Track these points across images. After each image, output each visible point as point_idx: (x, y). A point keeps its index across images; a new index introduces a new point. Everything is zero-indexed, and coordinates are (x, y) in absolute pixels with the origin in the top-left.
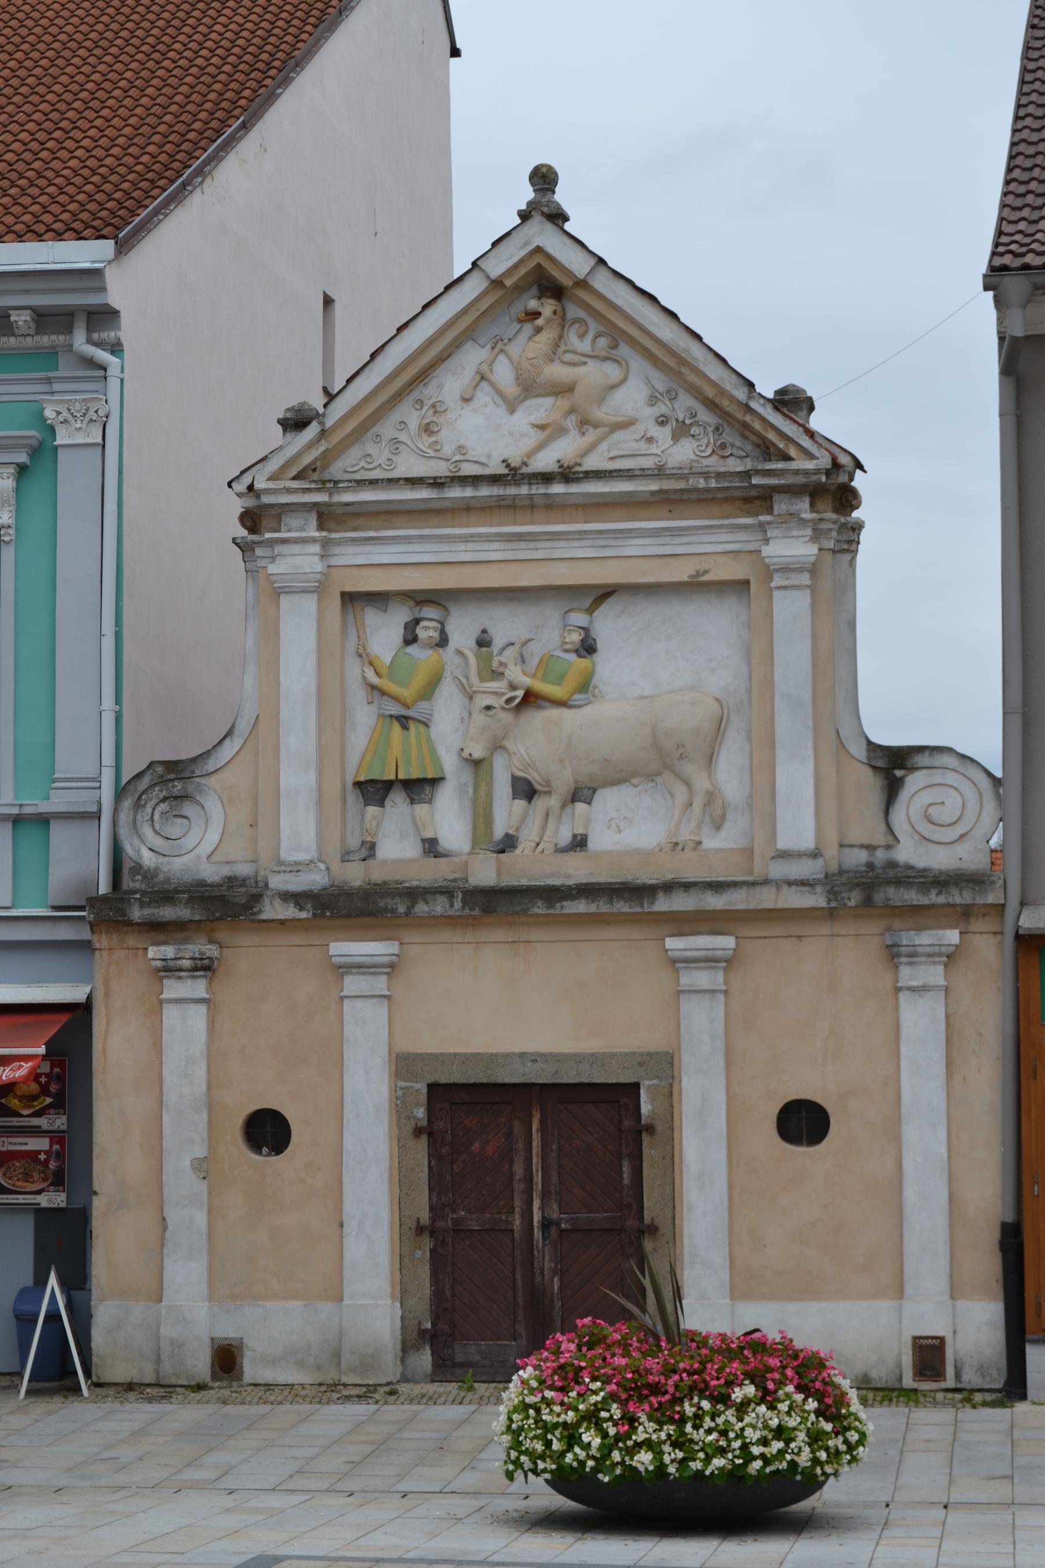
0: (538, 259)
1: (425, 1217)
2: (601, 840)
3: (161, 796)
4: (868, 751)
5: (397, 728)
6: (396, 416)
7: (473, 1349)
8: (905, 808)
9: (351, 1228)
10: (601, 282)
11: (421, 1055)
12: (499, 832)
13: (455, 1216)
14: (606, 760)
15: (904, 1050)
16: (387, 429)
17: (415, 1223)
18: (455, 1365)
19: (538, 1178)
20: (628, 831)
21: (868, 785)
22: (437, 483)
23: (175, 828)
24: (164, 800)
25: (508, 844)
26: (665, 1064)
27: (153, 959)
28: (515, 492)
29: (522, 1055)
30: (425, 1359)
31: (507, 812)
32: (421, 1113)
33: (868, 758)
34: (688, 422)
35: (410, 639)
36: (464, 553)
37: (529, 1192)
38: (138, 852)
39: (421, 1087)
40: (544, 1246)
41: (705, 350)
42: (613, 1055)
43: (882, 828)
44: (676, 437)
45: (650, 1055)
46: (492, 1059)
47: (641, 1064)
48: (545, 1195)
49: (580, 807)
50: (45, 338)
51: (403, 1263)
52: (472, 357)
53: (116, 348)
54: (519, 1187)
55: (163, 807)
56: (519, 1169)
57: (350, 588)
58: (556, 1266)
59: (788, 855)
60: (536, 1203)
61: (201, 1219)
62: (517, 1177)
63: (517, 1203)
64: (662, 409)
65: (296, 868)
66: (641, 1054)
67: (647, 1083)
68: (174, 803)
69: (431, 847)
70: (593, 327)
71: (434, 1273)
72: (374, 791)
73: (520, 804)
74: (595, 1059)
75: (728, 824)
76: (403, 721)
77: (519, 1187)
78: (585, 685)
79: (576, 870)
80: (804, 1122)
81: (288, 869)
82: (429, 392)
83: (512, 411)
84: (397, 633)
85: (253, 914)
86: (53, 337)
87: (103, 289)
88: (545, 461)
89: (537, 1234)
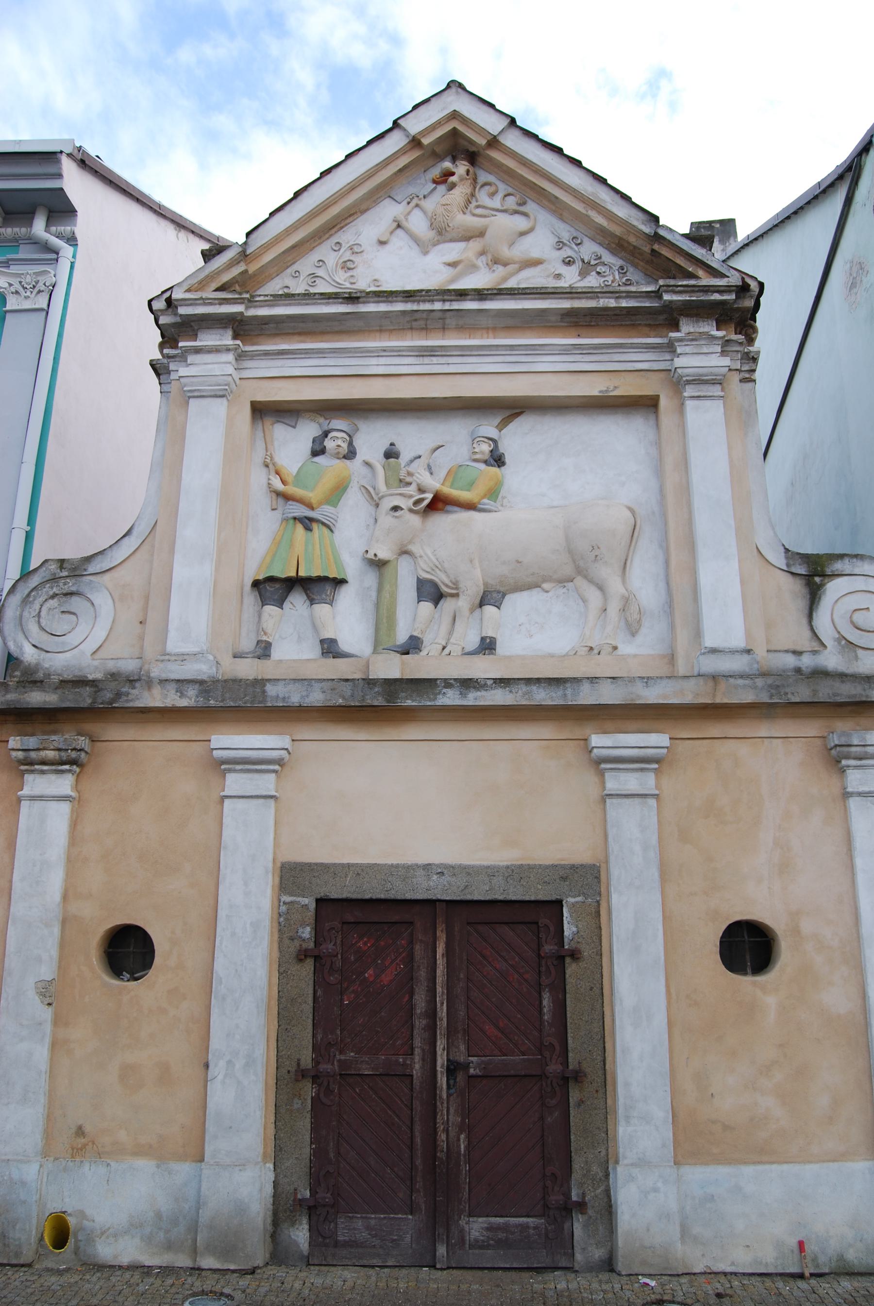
0: (454, 124)
1: (307, 1057)
3: (51, 593)
4: (787, 558)
5: (300, 528)
6: (314, 257)
7: (359, 1224)
8: (829, 613)
9: (218, 1069)
10: (512, 140)
11: (310, 865)
12: (402, 637)
13: (343, 1057)
14: (518, 562)
15: (859, 862)
17: (295, 1064)
18: (336, 1244)
19: (443, 1012)
20: (538, 634)
21: (791, 590)
23: (60, 625)
24: (53, 597)
25: (412, 646)
26: (590, 878)
27: (13, 750)
29: (427, 867)
30: (300, 1235)
31: (411, 616)
32: (307, 932)
33: (788, 565)
34: (593, 262)
35: (318, 451)
36: (376, 366)
37: (432, 1028)
38: (21, 648)
39: (309, 901)
40: (449, 1095)
41: (612, 193)
42: (531, 867)
43: (807, 633)
44: (583, 274)
45: (573, 868)
47: (564, 879)
48: (451, 1033)
49: (489, 610)
50: (9, 230)
51: (281, 1113)
52: (388, 211)
53: (72, 240)
54: (420, 1023)
55: (53, 603)
56: (420, 1001)
57: (260, 398)
58: (463, 1120)
59: (721, 651)
61: (41, 1054)
62: (418, 1011)
63: (417, 1042)
64: (567, 252)
66: (563, 867)
67: (571, 900)
68: (64, 599)
69: (330, 648)
70: (503, 188)
71: (315, 1128)
72: (274, 588)
73: (427, 607)
75: (644, 630)
76: (307, 523)
77: (420, 1023)
78: (493, 493)
80: (748, 947)
81: (173, 658)
82: (346, 237)
83: (425, 253)
84: (307, 446)
85: (127, 701)
86: (16, 230)
87: (59, 176)
89: (442, 1080)
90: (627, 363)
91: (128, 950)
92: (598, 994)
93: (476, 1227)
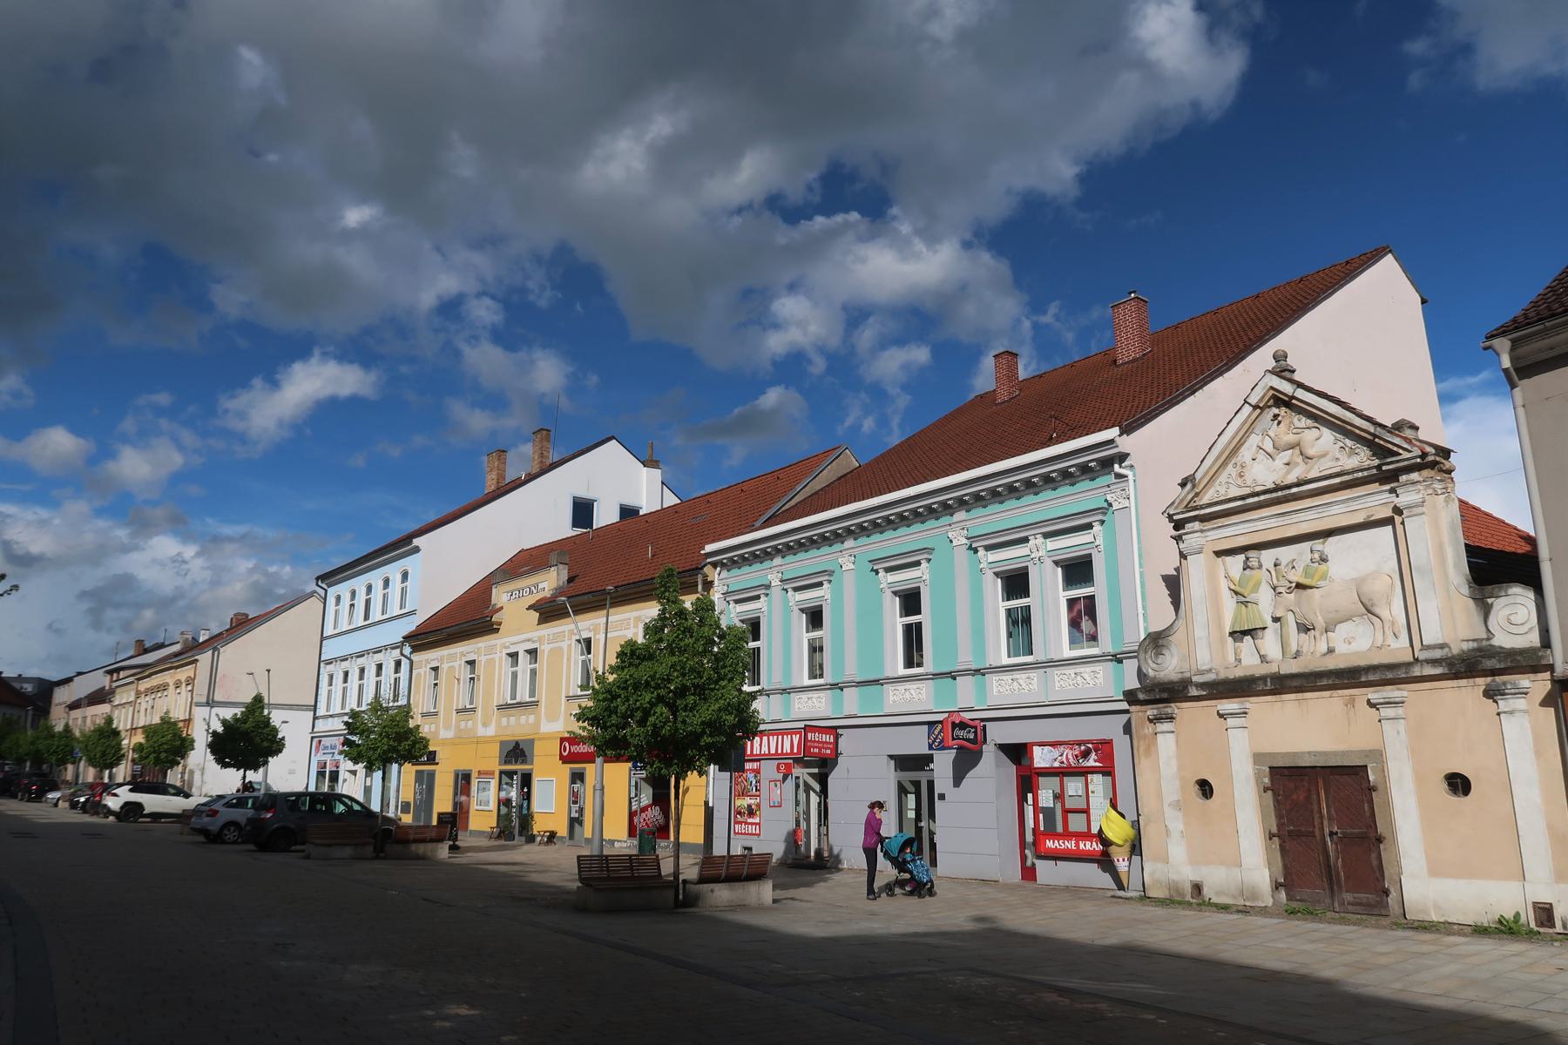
1: (1274, 830)
2: (1341, 648)
12: (1294, 648)
16: (1223, 478)
19: (1325, 812)
20: (1354, 643)
22: (1243, 498)
25: (1297, 655)
26: (1378, 755)
28: (1280, 495)
31: (1295, 639)
32: (1266, 780)
46: (1295, 755)
48: (1330, 819)
56: (1316, 808)
60: (1326, 823)
65: (1202, 673)
69: (1263, 658)
72: (1238, 635)
74: (1344, 754)
76: (1245, 603)
77: (1317, 816)
78: (1324, 577)
79: (1331, 664)
80: (1459, 784)
88: (1292, 479)
90: (1376, 501)
91: (1205, 788)
92: (1387, 804)
93: (1348, 897)
